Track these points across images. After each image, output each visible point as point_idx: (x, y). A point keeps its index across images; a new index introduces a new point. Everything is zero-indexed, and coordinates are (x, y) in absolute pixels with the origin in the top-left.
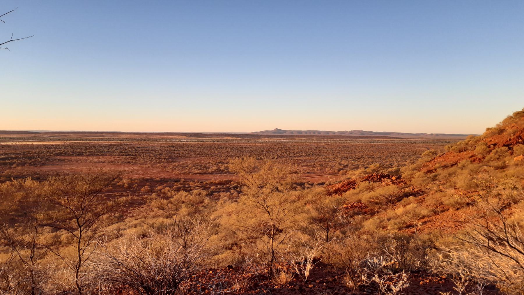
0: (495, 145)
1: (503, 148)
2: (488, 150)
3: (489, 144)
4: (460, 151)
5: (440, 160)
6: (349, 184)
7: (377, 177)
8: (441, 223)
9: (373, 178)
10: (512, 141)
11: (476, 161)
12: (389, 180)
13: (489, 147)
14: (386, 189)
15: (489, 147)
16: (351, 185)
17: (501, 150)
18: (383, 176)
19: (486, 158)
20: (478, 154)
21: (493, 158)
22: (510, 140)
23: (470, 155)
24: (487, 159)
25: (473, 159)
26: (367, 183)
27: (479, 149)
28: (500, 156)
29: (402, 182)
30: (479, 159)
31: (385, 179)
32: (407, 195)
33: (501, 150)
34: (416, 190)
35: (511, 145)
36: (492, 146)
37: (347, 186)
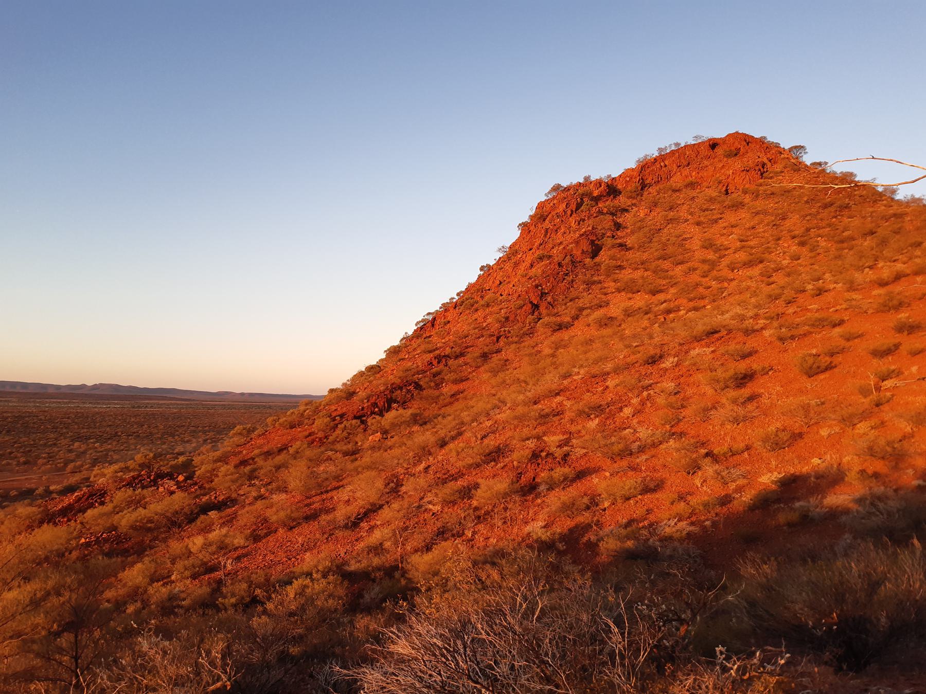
0: (342, 416)
1: (354, 421)
2: (332, 424)
3: (334, 414)
4: (292, 427)
5: (260, 441)
6: (91, 495)
7: (149, 477)
8: (265, 555)
9: (141, 481)
12: (172, 483)
13: (334, 419)
14: (167, 501)
16: (98, 496)
17: (351, 425)
18: (160, 476)
21: (341, 437)
22: (363, 409)
23: (307, 433)
25: (311, 440)
26: (130, 491)
27: (321, 422)
28: (349, 434)
29: (196, 484)
30: (320, 439)
31: (166, 480)
32: (205, 509)
33: (351, 425)
34: (221, 498)
37: (88, 498)
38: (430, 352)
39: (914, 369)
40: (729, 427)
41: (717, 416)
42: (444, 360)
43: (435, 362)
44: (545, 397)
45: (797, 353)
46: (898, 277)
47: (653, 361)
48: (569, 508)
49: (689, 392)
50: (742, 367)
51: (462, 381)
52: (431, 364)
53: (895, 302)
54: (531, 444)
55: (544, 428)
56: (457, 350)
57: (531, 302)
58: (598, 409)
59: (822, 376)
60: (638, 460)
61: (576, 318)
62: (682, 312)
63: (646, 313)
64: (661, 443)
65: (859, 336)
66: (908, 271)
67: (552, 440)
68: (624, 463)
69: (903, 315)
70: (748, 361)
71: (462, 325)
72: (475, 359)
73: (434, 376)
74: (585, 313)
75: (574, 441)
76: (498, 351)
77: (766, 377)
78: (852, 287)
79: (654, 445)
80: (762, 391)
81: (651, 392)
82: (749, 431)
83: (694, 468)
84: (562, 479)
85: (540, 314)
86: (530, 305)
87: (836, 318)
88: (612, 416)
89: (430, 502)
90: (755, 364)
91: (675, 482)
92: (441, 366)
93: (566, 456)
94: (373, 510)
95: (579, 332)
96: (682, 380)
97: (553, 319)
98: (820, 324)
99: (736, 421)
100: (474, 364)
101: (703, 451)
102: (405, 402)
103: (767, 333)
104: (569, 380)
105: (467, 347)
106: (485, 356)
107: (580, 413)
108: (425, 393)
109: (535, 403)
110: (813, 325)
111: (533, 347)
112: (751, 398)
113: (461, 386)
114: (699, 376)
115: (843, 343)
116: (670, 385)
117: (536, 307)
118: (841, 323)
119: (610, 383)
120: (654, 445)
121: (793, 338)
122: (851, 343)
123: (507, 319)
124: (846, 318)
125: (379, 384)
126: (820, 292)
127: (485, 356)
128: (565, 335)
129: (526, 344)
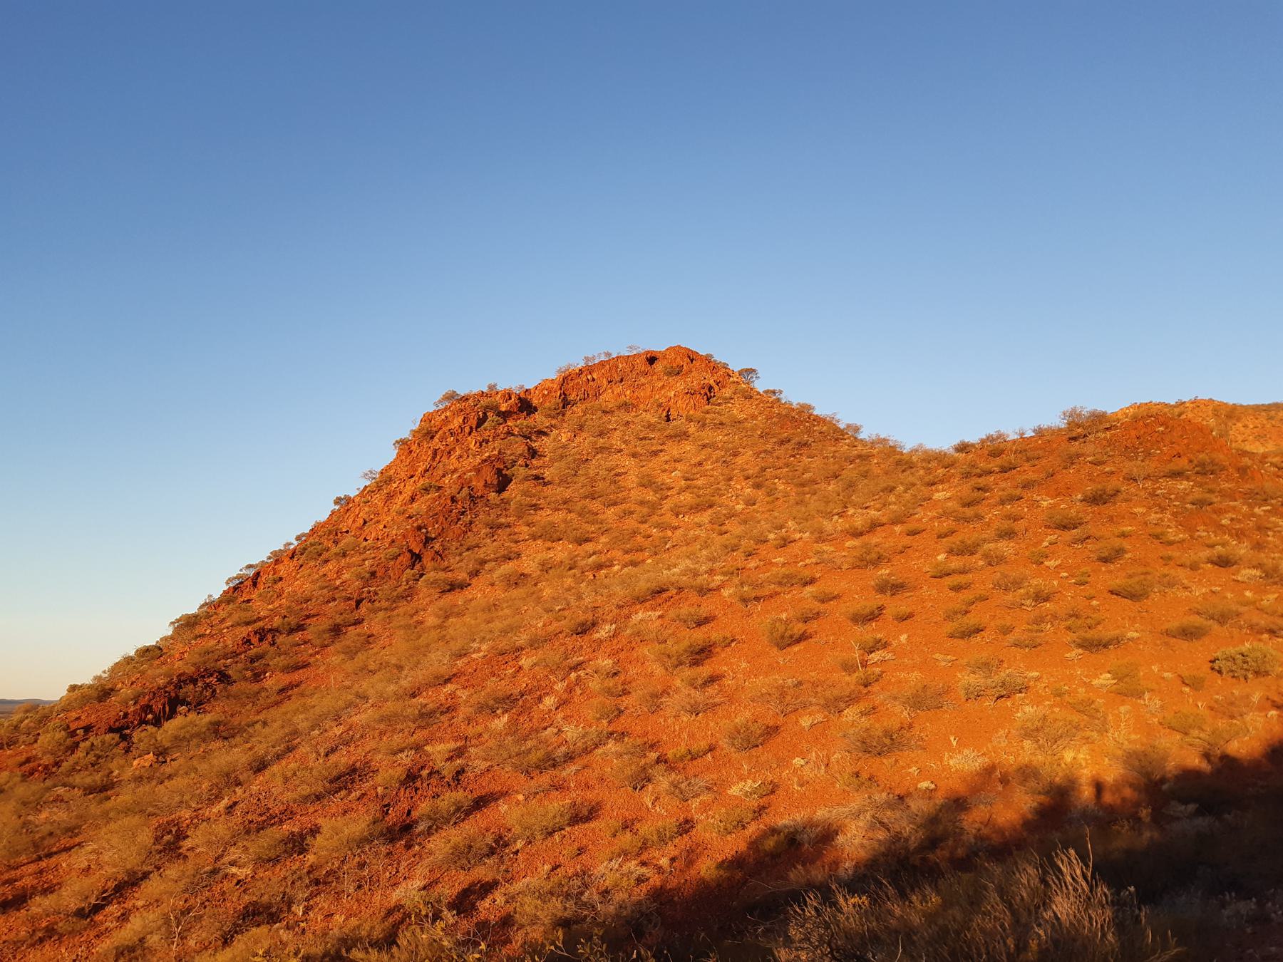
0: (87, 729)
1: (108, 737)
2: (69, 741)
3: (73, 727)
10: (130, 718)
11: (36, 775)
15: (73, 734)
19: (65, 764)
20: (44, 753)
21: (82, 763)
22: (126, 715)
24: (66, 765)
28: (99, 757)
30: (46, 767)
33: (103, 743)
35: (128, 728)
36: (80, 732)
38: (248, 624)
39: (903, 638)
40: (685, 719)
41: (671, 704)
42: (269, 636)
43: (255, 640)
44: (430, 685)
45: (765, 618)
46: (874, 526)
47: (584, 629)
48: (464, 855)
49: (633, 671)
50: (699, 636)
51: (297, 667)
52: (247, 641)
53: (874, 556)
54: (406, 758)
55: (426, 732)
56: (293, 620)
57: (410, 551)
58: (507, 702)
59: (796, 648)
60: (564, 774)
61: (475, 574)
62: (616, 568)
63: (570, 569)
64: (596, 747)
65: (835, 598)
66: (884, 520)
67: (438, 751)
68: (545, 779)
69: (884, 572)
70: (705, 628)
71: (303, 583)
72: (320, 634)
73: (252, 661)
74: (487, 567)
75: (472, 750)
76: (358, 622)
77: (728, 650)
78: (821, 537)
79: (587, 751)
80: (725, 668)
81: (582, 673)
82: (712, 724)
83: (642, 780)
84: (452, 809)
85: (423, 568)
86: (409, 555)
87: (807, 574)
88: (526, 710)
89: (233, 863)
90: (712, 633)
91: (616, 802)
92: (265, 645)
93: (460, 772)
94: (133, 881)
95: (478, 593)
96: (622, 656)
97: (442, 575)
98: (788, 581)
99: (695, 710)
100: (318, 642)
101: (653, 755)
102: (200, 703)
103: (726, 593)
104: (465, 660)
105: (308, 617)
106: (336, 630)
107: (481, 708)
108: (234, 688)
109: (414, 696)
110: (780, 583)
111: (412, 616)
112: (713, 679)
113: (296, 676)
114: (645, 650)
115: (818, 606)
116: (606, 663)
117: (416, 557)
118: (812, 581)
119: (525, 662)
120: (587, 751)
121: (757, 599)
122: (826, 605)
123: (373, 574)
124: (818, 575)
125: (158, 676)
126: (785, 542)
127: (336, 630)
128: (459, 598)
129: (401, 611)
